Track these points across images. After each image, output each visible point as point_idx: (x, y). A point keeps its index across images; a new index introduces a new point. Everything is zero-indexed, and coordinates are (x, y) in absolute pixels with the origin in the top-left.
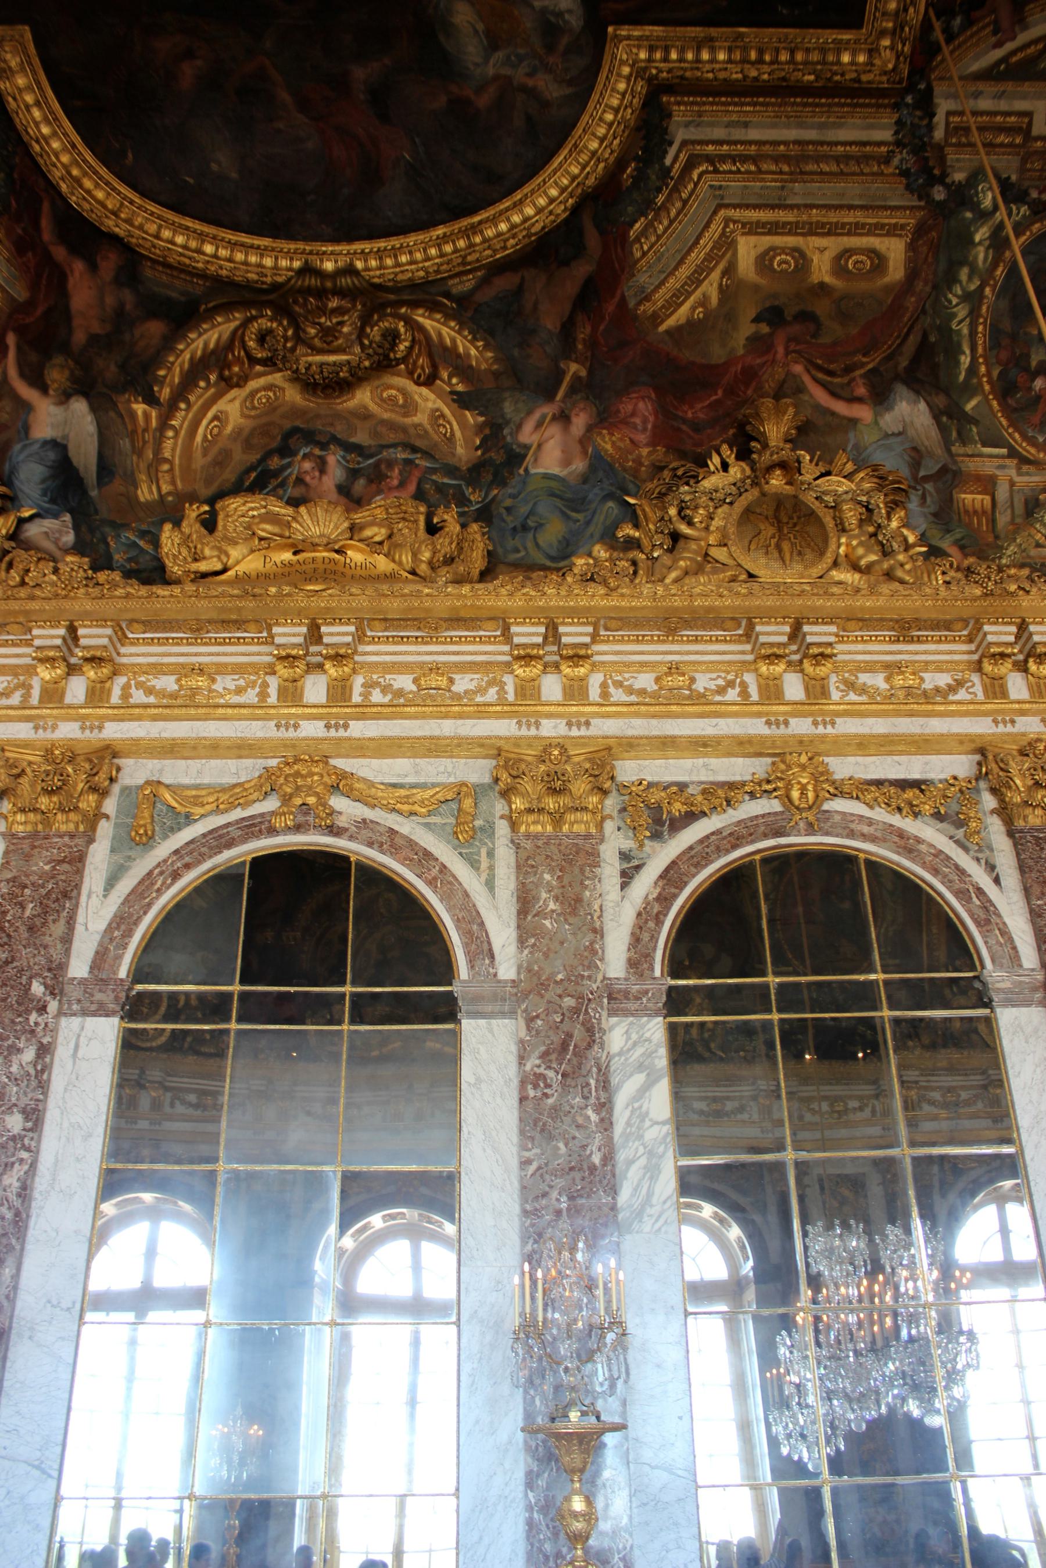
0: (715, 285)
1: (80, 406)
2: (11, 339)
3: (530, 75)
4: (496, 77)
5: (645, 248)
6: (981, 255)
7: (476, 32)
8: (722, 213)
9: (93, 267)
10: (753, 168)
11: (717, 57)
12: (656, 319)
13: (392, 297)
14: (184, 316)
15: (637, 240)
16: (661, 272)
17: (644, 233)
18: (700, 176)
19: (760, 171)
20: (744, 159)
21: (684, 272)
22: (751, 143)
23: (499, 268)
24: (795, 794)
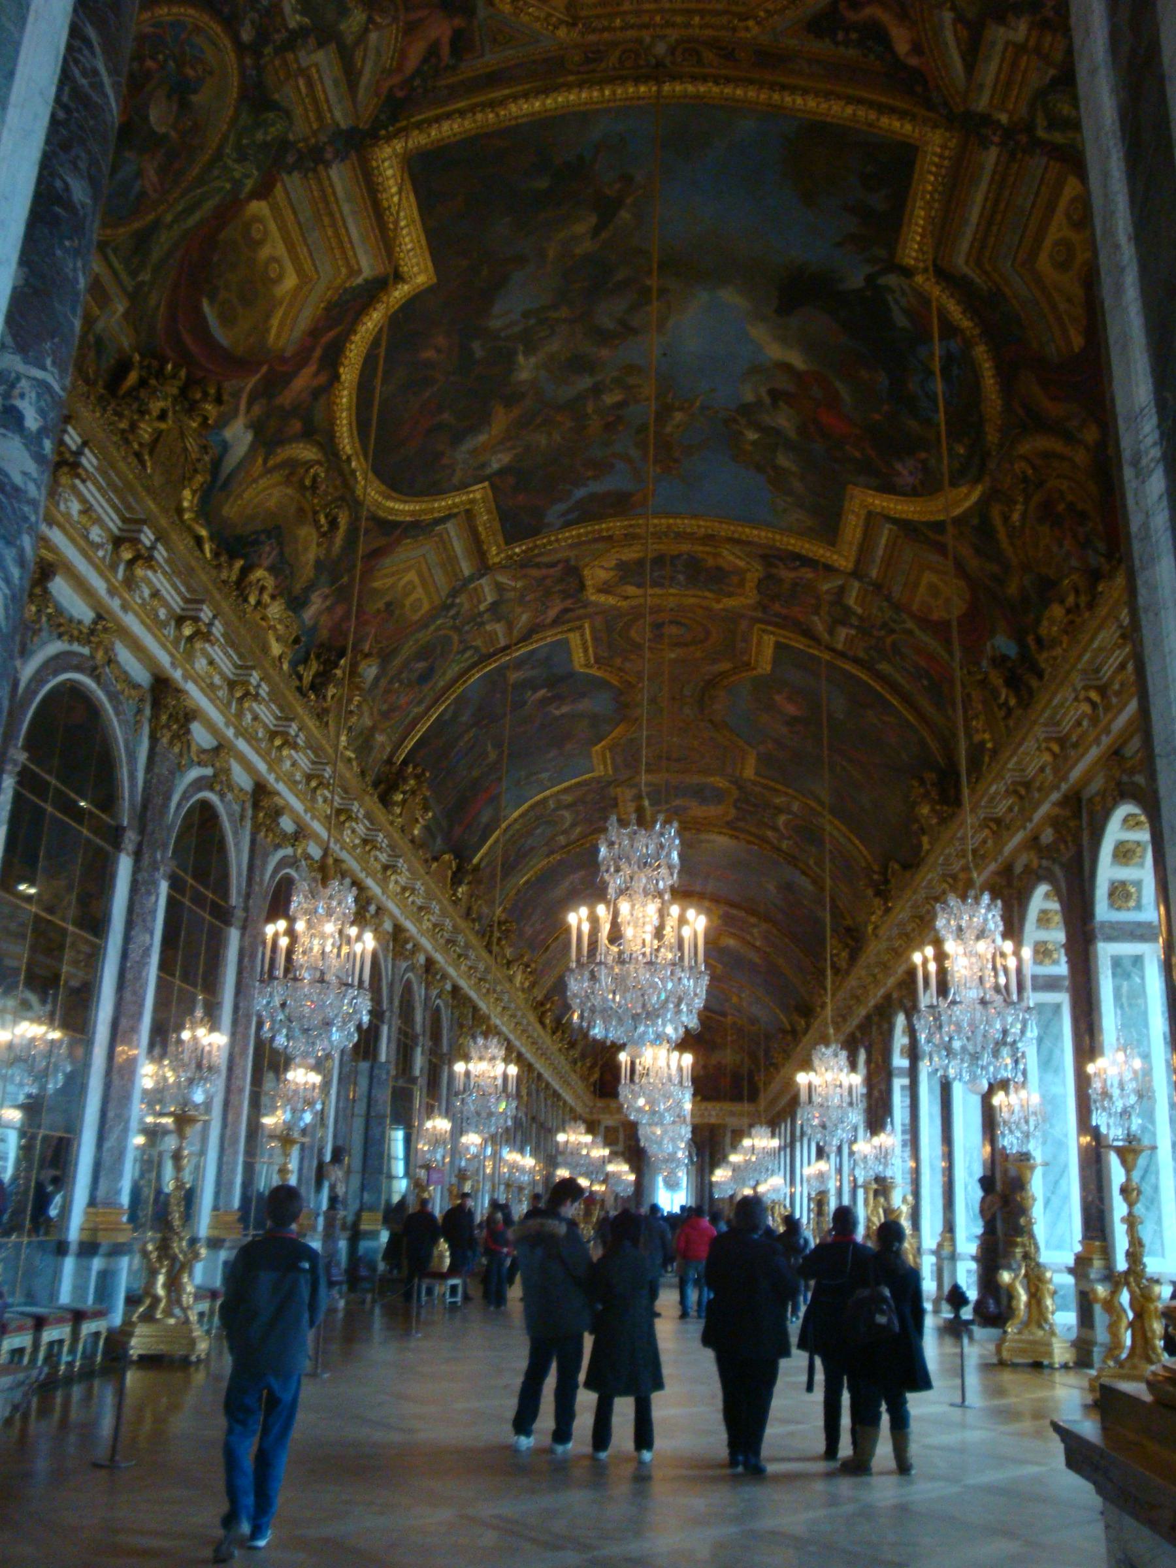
1: (249, 437)
2: (264, 369)
6: (432, 628)
9: (316, 374)
14: (308, 434)
24: (300, 851)
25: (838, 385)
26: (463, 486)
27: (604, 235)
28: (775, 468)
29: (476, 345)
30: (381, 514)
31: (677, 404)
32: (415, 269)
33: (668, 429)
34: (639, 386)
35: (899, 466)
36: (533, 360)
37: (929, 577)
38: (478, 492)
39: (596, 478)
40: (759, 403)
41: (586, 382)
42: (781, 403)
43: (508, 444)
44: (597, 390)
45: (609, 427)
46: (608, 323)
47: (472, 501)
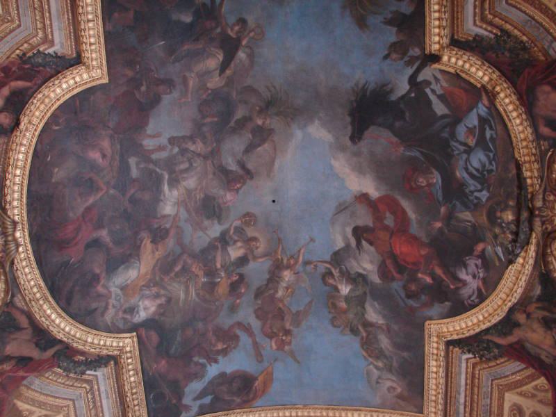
0: (40, 414)
3: (114, 306)
4: (110, 292)
5: (50, 377)
7: (127, 281)
8: (71, 403)
10: (91, 407)
11: (132, 378)
12: (20, 397)
13: (8, 269)
15: (53, 372)
16: (41, 389)
17: (57, 374)
18: (85, 388)
19: (90, 410)
20: (94, 402)
21: (42, 398)
22: (101, 402)
23: (30, 316)
25: (406, 204)
26: (113, 329)
27: (228, 72)
28: (367, 324)
29: (132, 161)
30: (35, 310)
31: (285, 261)
32: (94, 63)
33: (280, 293)
34: (255, 239)
35: (463, 275)
36: (175, 193)
37: (510, 398)
38: (128, 342)
39: (225, 352)
40: (348, 246)
41: (215, 230)
42: (364, 243)
43: (155, 290)
44: (224, 240)
45: (234, 287)
46: (233, 166)
47: (121, 350)
